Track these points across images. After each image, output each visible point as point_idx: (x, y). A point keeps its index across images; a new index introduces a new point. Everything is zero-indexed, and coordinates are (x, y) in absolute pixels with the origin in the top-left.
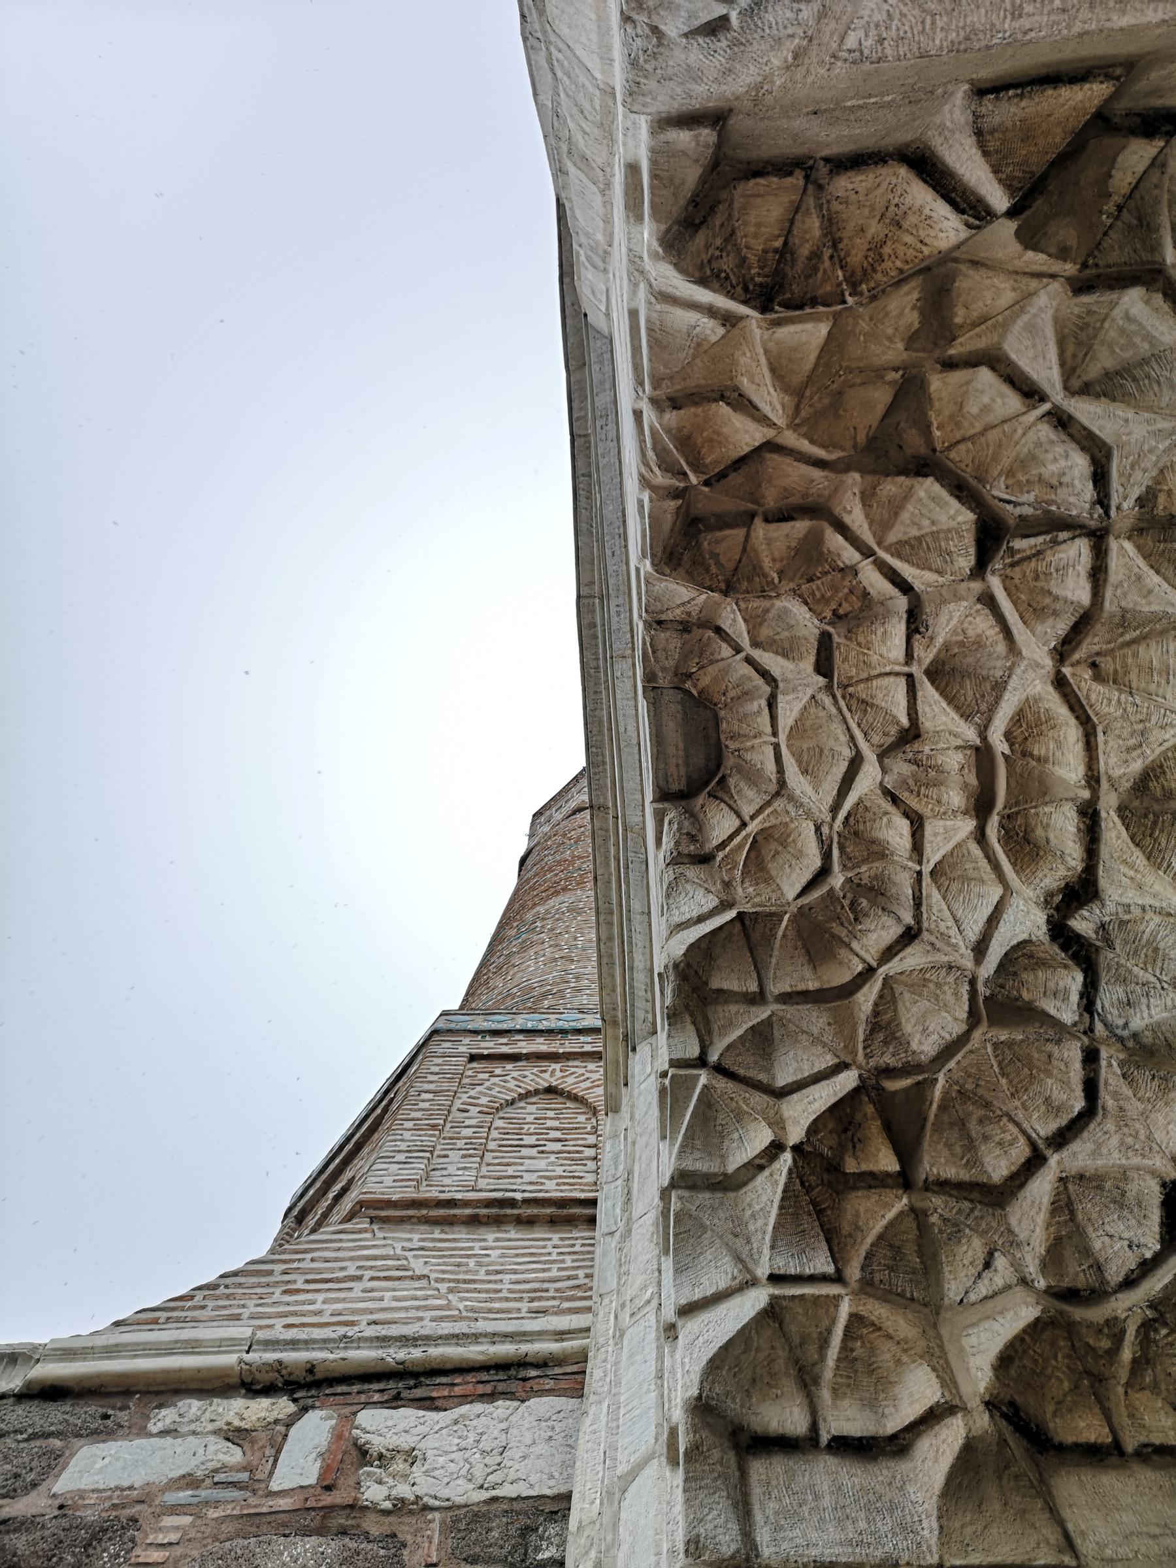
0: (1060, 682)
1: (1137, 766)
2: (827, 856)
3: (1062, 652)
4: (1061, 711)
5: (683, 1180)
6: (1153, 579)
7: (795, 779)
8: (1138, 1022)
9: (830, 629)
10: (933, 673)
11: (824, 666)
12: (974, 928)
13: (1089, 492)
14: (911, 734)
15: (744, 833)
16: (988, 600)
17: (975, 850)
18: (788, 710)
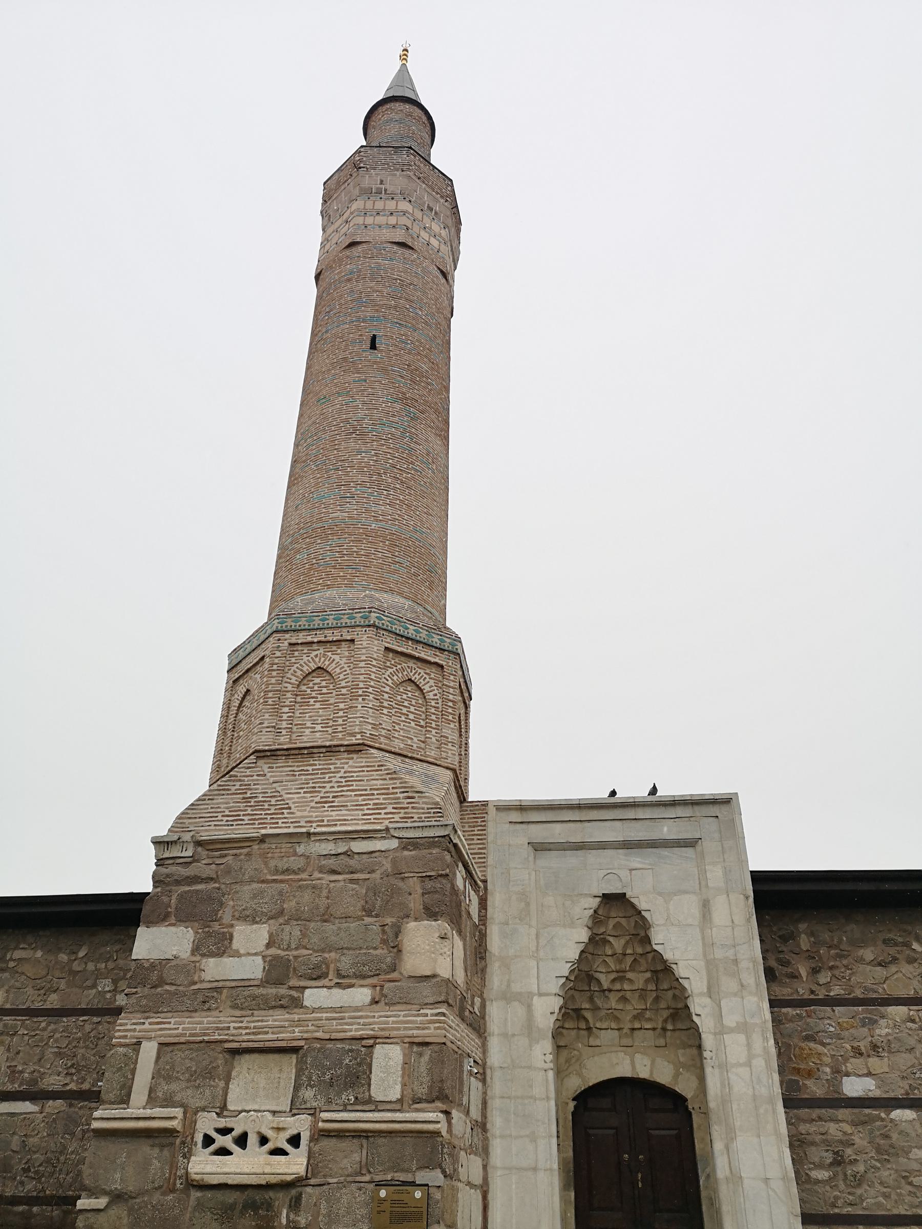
0: (638, 989)
1: (628, 998)
2: (601, 935)
3: (642, 990)
4: (634, 989)
5: (567, 978)
6: (651, 999)
7: (612, 923)
8: (596, 999)
9: (639, 937)
10: (635, 959)
11: (633, 935)
12: (599, 970)
13: (662, 989)
14: (625, 955)
15: (600, 917)
16: (647, 971)
17: (610, 970)
18: (623, 921)
